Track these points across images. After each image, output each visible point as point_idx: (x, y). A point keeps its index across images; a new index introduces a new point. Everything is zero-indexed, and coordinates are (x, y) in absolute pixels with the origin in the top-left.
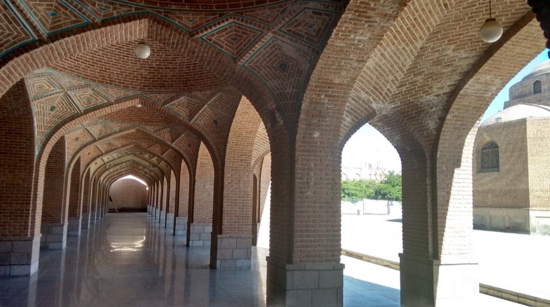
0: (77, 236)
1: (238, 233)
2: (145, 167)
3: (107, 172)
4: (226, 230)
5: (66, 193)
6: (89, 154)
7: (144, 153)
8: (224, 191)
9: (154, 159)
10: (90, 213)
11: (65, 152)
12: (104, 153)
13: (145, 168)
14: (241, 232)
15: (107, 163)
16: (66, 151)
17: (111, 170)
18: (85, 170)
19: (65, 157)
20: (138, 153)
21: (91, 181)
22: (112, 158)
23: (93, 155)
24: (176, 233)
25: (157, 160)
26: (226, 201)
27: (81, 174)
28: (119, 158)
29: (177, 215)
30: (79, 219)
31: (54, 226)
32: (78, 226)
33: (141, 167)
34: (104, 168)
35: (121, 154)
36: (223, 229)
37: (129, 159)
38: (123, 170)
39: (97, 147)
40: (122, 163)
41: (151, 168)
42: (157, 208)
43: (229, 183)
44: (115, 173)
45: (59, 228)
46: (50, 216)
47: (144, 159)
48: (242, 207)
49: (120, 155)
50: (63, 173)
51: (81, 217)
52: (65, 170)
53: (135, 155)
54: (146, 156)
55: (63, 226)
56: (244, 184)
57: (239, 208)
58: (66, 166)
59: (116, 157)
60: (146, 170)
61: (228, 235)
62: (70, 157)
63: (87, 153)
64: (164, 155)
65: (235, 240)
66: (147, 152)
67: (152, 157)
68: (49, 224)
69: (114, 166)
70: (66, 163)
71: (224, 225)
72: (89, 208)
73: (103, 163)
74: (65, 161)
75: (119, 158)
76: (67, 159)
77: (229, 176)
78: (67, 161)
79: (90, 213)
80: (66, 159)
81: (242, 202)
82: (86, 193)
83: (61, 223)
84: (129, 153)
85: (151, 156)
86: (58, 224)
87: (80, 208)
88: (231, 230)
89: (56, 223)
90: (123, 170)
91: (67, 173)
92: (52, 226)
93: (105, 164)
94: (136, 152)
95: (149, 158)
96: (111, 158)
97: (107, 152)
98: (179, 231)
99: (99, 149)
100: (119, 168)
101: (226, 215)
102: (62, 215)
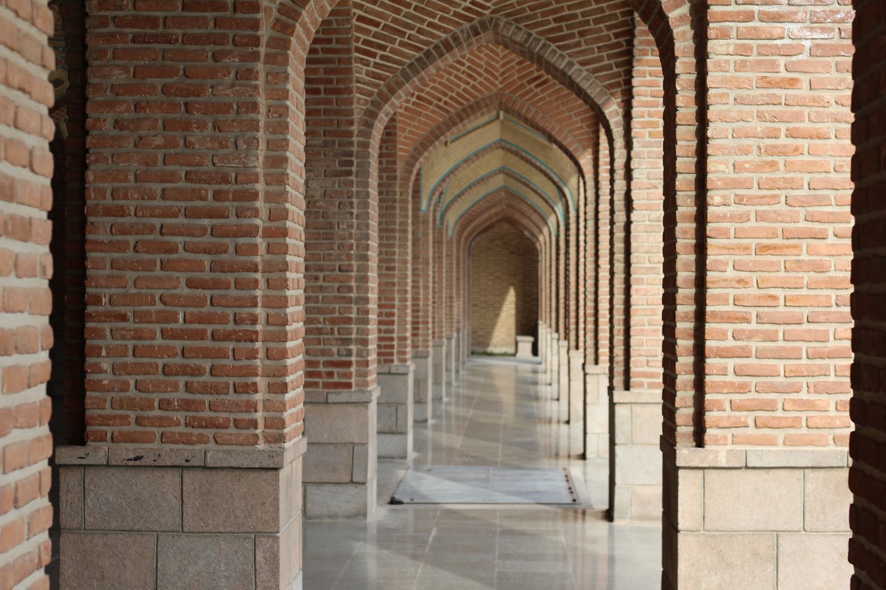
1: (188, 440)
4: (106, 420)
8: (90, 176)
14: (209, 432)
26: (103, 236)
36: (91, 412)
43: (117, 124)
48: (207, 275)
56: (216, 127)
57: (190, 284)
61: (126, 451)
65: (172, 477)
71: (98, 386)
77: (119, 77)
81: (207, 239)
88: (139, 421)
101: (107, 327)
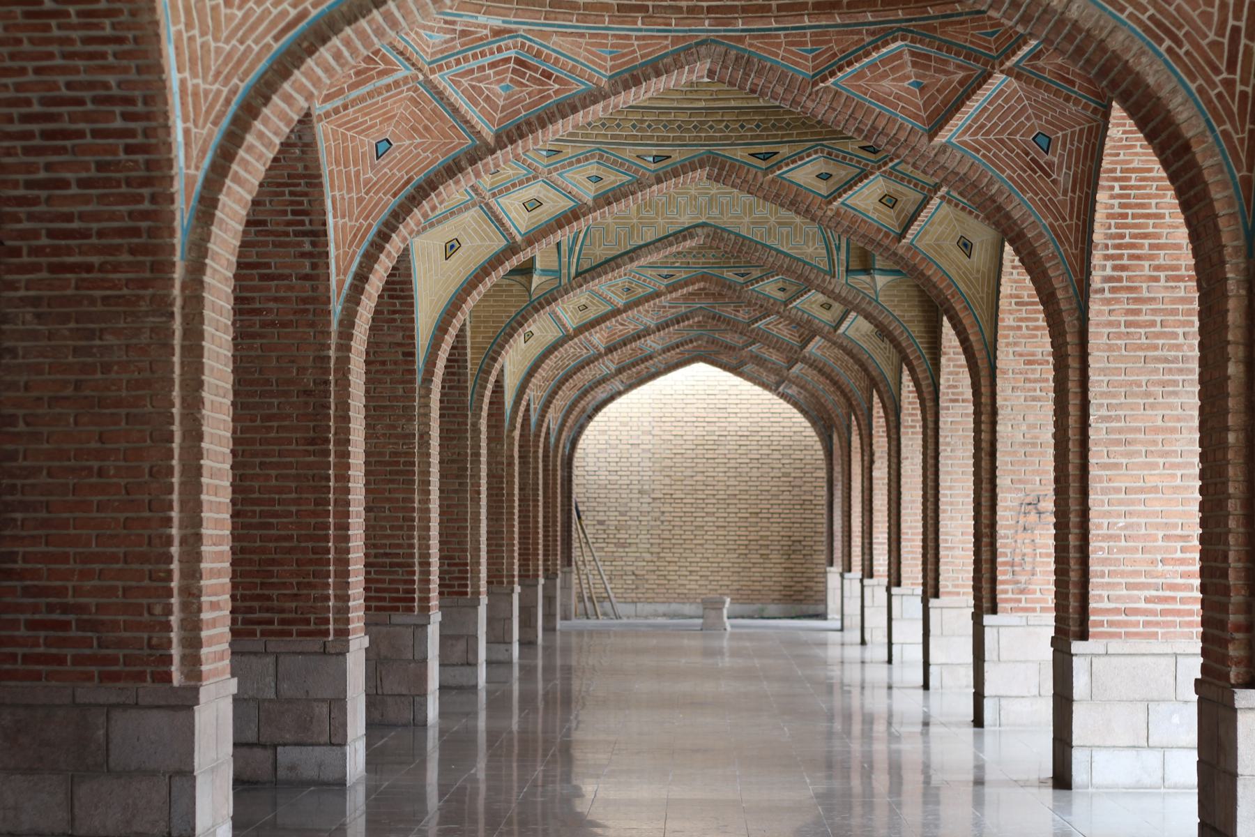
0: (340, 784)
2: (802, 278)
3: (541, 329)
5: (194, 435)
6: (383, 148)
7: (785, 150)
9: (866, 197)
10: (436, 617)
11: (162, 86)
12: (488, 133)
13: (806, 285)
15: (531, 240)
16: (174, 78)
17: (568, 311)
18: (362, 278)
19: (167, 129)
20: (740, 154)
21: (428, 380)
22: (566, 204)
23: (416, 154)
24: (1079, 773)
25: (889, 201)
27: (336, 307)
28: (606, 199)
29: (1073, 622)
30: (343, 653)
31: (124, 707)
32: (338, 703)
33: (770, 288)
34: (512, 283)
35: (619, 164)
37: (686, 220)
38: (645, 316)
39: (440, 95)
40: (632, 254)
41: (840, 282)
42: (895, 579)
44: (598, 338)
45: (157, 720)
46: (94, 625)
47: (794, 200)
49: (613, 179)
50: (163, 268)
51: (359, 643)
52: (179, 240)
53: (722, 171)
54: (805, 174)
55: (187, 701)
58: (183, 210)
59: (588, 193)
60: (811, 303)
62: (211, 133)
63: (367, 144)
64: (959, 121)
66: (817, 133)
67: (849, 185)
68: (89, 693)
69: (586, 274)
70: (178, 186)
72: (426, 581)
73: (499, 243)
74: (170, 163)
75: (606, 199)
76: (188, 143)
78: (187, 168)
79: (436, 617)
80: (179, 153)
82: (392, 471)
83: (177, 679)
84: (678, 156)
85: (842, 173)
86: (148, 690)
87: (344, 574)
89: (140, 677)
90: (645, 316)
91: (197, 268)
92: (111, 707)
93: (512, 249)
94: (728, 152)
95: (823, 188)
96: (556, 204)
97: (512, 134)
98: (1100, 757)
99: (455, 110)
100: (620, 302)
102: (174, 619)
